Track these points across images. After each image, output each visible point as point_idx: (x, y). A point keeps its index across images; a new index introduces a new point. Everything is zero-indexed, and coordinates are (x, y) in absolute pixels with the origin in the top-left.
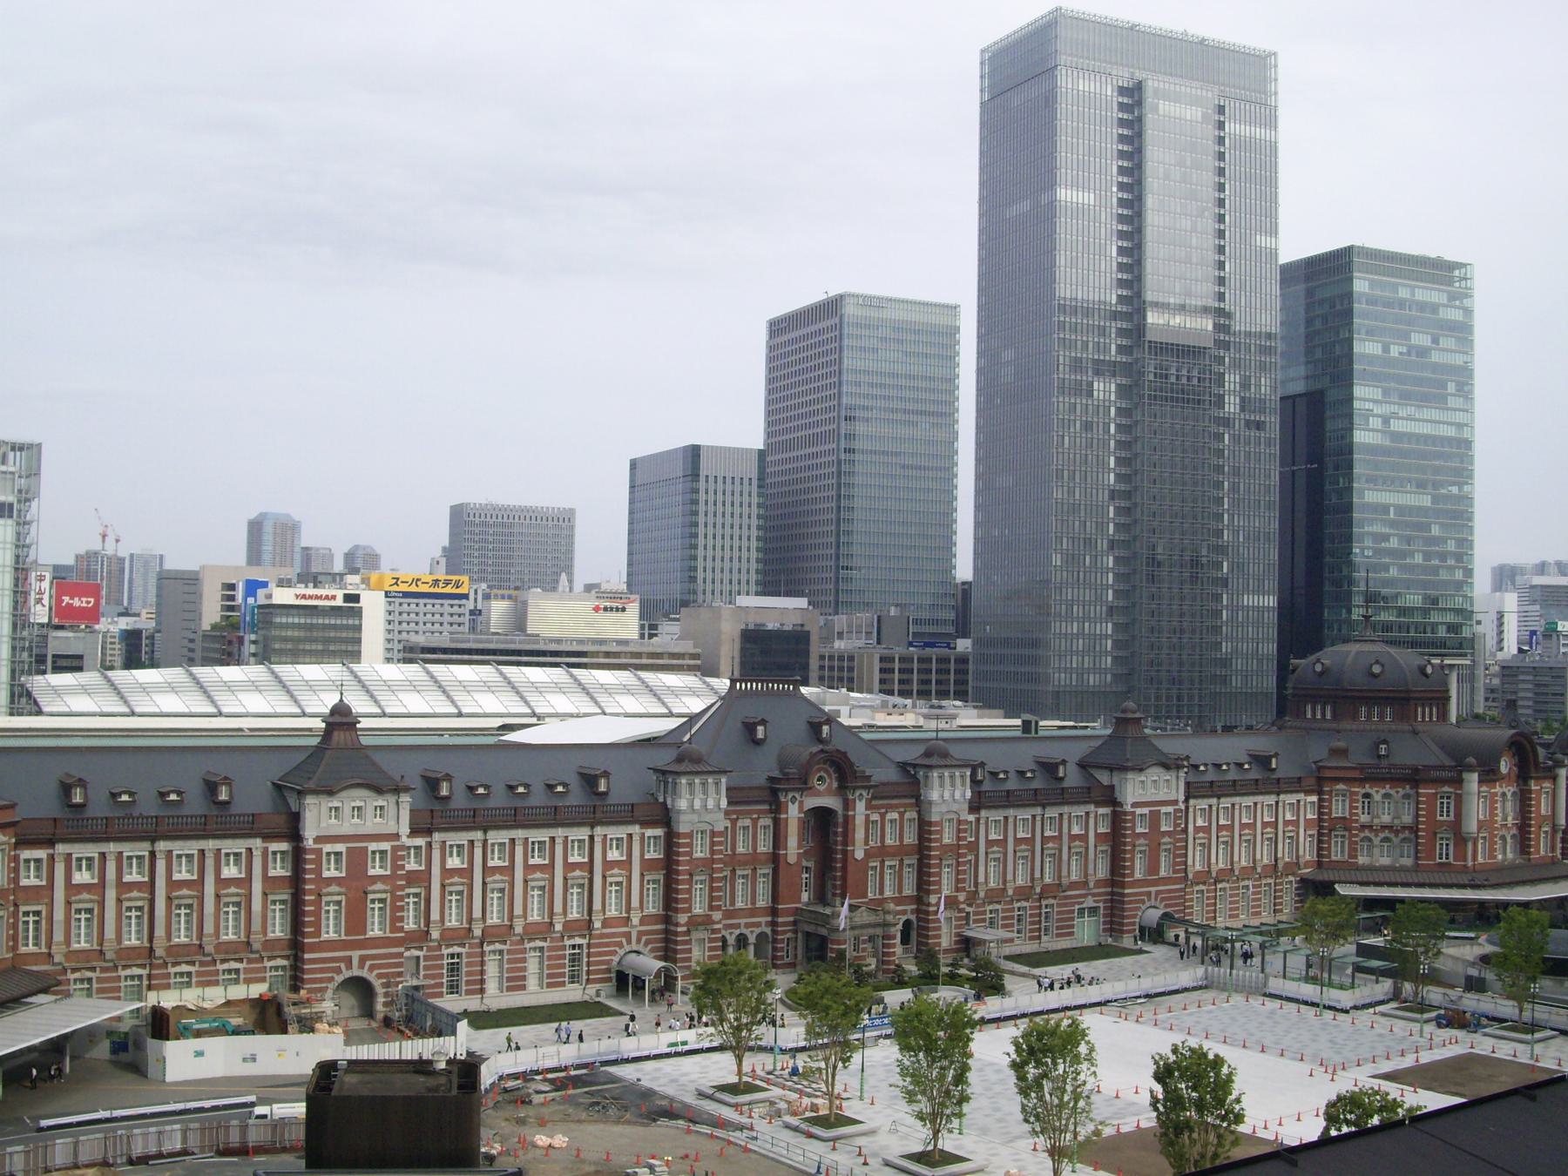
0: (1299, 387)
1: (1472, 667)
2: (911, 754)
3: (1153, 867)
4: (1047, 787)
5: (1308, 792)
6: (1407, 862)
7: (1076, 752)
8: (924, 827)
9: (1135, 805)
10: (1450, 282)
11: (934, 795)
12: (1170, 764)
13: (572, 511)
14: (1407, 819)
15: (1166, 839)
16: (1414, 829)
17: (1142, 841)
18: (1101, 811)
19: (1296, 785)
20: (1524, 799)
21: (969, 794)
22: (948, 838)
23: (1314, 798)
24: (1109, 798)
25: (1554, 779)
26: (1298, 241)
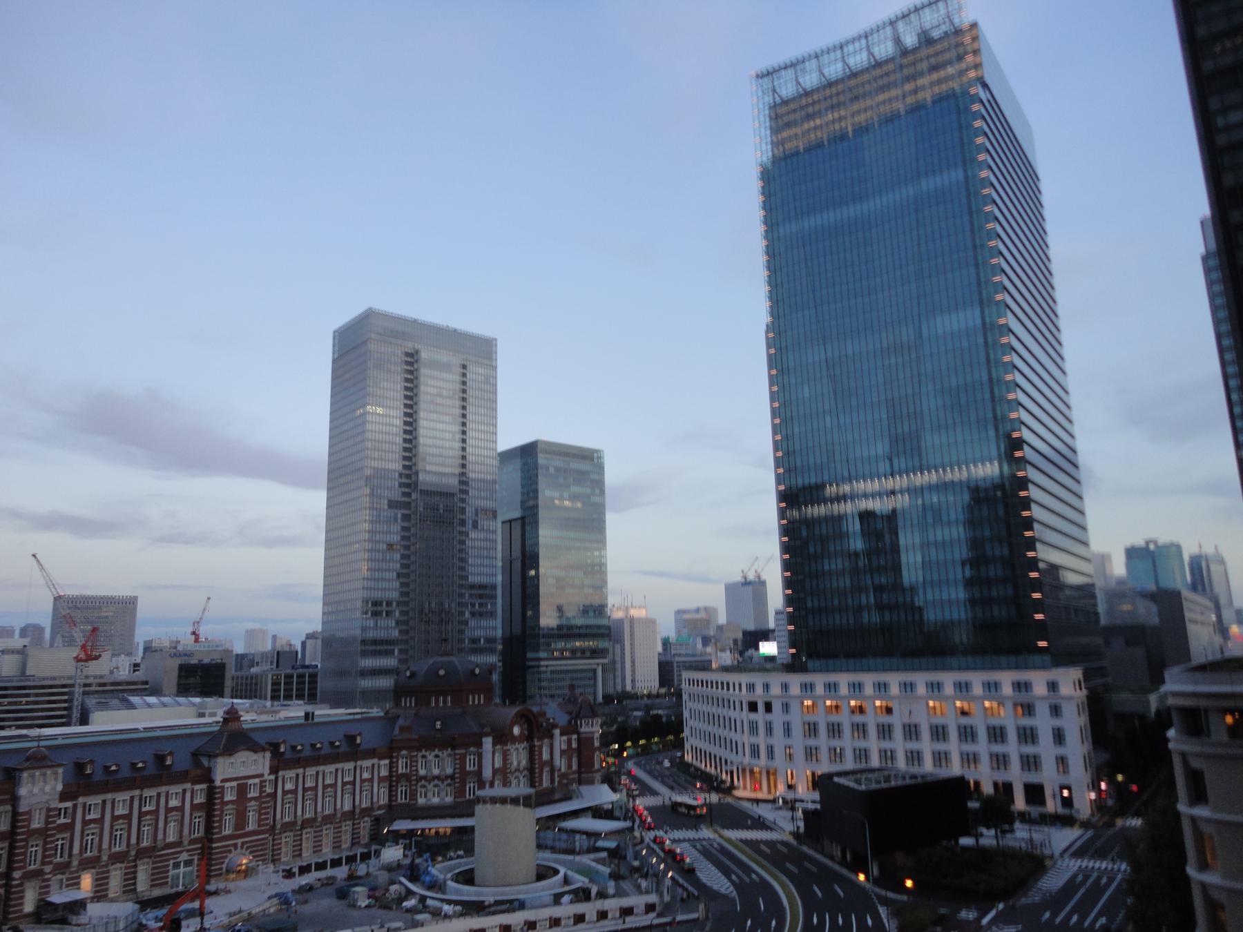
0: (517, 514)
1: (614, 662)
2: (11, 763)
3: (241, 821)
4: (161, 773)
5: (380, 758)
6: (449, 799)
7: (195, 745)
8: (15, 814)
9: (222, 781)
10: (592, 459)
11: (23, 791)
12: (255, 748)
13: (136, 598)
14: (449, 771)
15: (253, 803)
16: (452, 777)
17: (230, 806)
18: (197, 787)
19: (371, 753)
20: (532, 753)
21: (60, 787)
22: (36, 824)
23: (387, 762)
24: (207, 777)
25: (551, 737)
26: (509, 437)
